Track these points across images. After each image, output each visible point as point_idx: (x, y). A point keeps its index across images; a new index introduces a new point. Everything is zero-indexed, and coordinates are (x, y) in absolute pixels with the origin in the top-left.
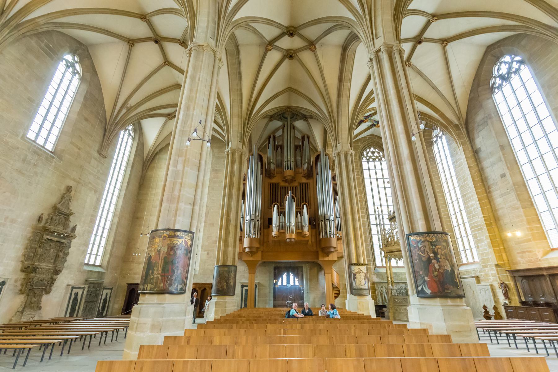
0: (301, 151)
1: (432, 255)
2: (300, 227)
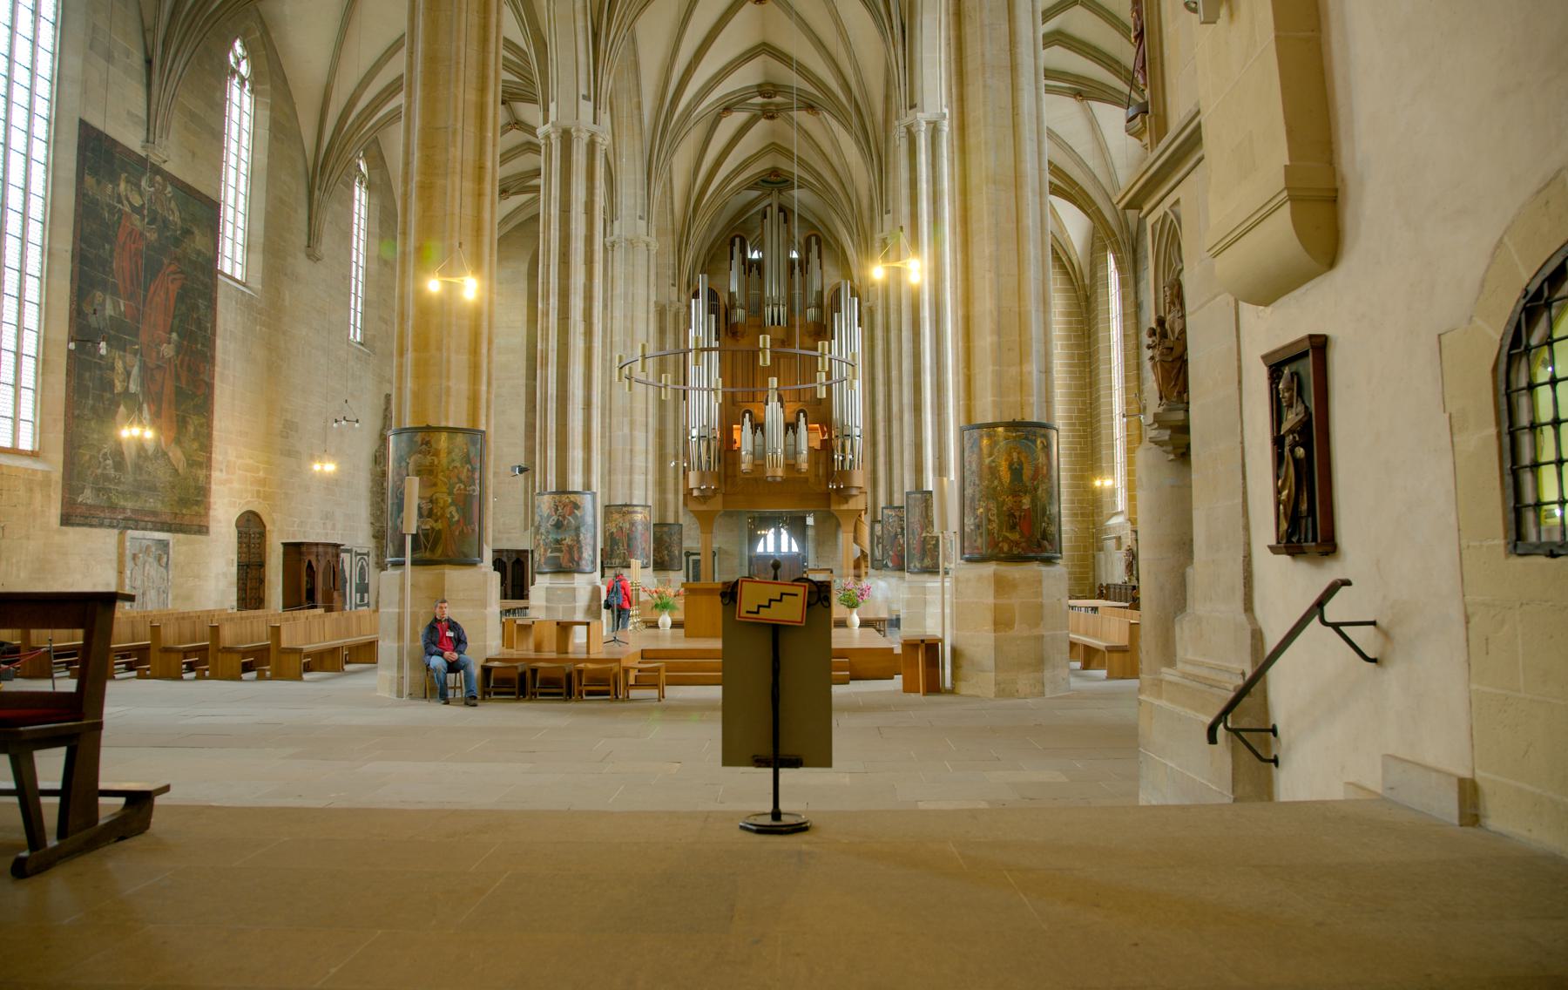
0: (803, 275)
1: (899, 530)
2: (792, 454)
